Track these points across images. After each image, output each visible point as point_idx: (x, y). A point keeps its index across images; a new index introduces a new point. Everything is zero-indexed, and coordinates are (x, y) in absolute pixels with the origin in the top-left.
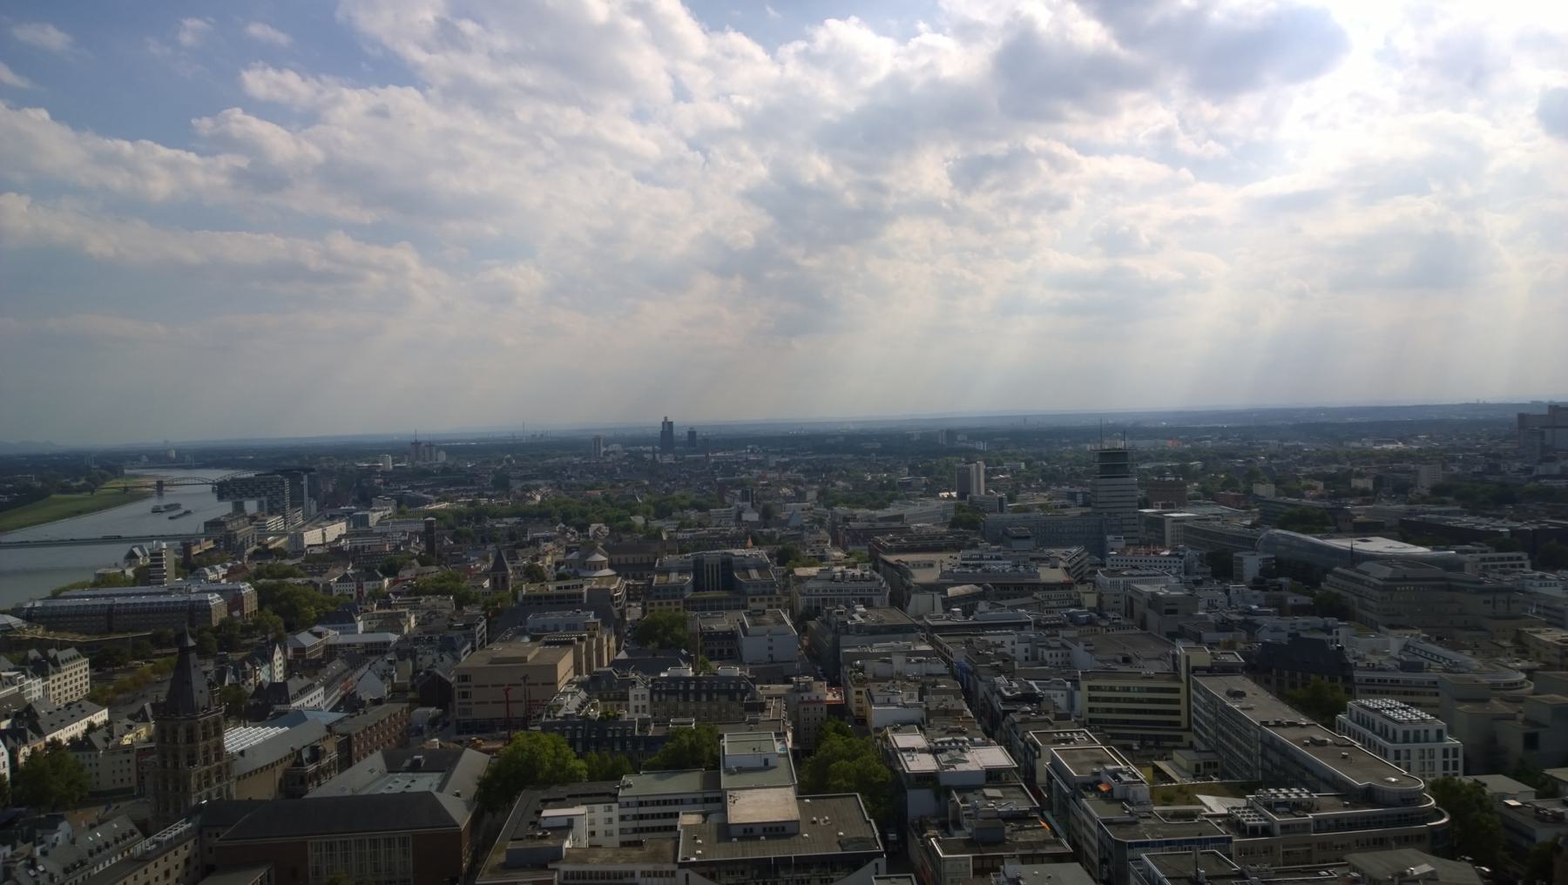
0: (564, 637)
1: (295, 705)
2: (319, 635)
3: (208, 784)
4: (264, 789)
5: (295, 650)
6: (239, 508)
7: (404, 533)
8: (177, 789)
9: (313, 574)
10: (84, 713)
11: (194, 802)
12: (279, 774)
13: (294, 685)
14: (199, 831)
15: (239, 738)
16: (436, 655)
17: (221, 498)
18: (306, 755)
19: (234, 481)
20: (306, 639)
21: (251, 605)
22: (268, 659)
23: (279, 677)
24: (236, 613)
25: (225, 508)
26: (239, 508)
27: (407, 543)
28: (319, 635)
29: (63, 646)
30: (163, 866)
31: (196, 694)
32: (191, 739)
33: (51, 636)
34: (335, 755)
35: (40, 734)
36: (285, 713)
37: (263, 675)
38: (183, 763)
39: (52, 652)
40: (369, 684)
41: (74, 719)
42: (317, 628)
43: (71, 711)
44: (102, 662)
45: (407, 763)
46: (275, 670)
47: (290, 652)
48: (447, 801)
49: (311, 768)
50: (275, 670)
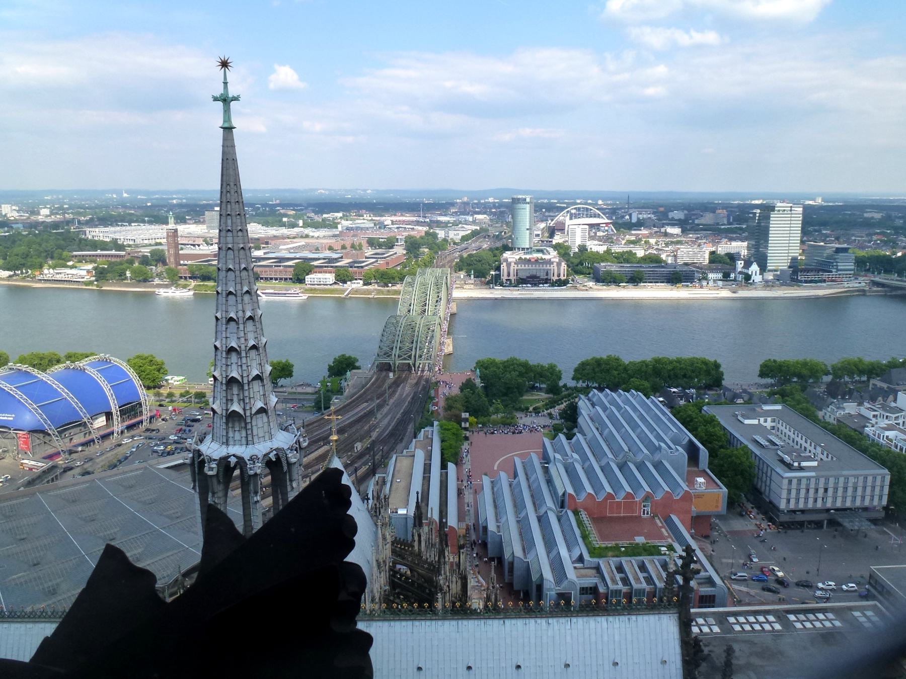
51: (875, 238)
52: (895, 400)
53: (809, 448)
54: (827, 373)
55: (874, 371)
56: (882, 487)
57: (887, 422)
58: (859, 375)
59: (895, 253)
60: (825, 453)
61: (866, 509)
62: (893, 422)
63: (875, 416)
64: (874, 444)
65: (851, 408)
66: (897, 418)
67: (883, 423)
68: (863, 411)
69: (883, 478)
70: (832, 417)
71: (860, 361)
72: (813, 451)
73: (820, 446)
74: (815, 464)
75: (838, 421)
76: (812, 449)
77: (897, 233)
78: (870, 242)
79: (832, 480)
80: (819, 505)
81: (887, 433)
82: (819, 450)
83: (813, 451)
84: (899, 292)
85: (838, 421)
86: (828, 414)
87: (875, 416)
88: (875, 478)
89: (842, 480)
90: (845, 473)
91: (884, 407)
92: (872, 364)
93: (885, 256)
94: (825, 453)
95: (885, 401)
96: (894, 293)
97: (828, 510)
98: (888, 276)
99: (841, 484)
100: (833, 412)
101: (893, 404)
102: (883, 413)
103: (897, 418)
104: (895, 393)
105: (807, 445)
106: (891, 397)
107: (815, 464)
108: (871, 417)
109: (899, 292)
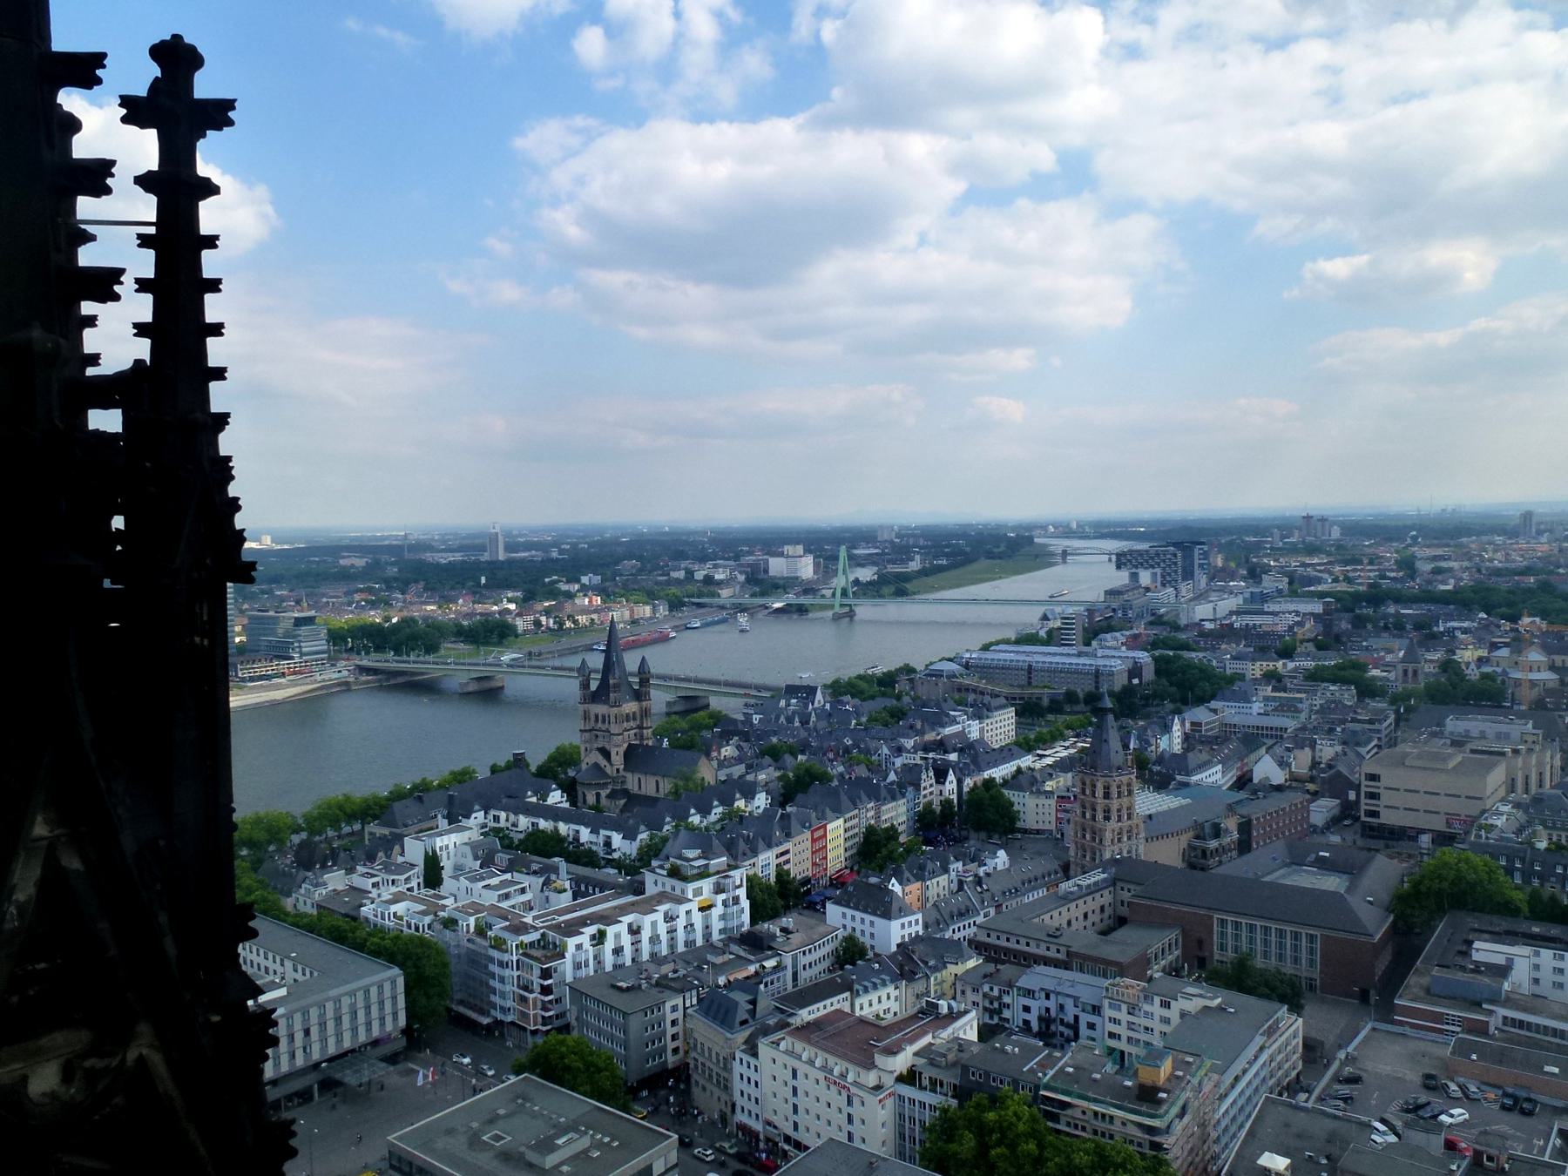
0: (1496, 747)
1: (1195, 778)
2: (1215, 711)
3: (1119, 840)
4: (1169, 853)
5: (1193, 724)
6: (1134, 577)
7: (1297, 613)
8: (1094, 839)
9: (1206, 650)
10: (1012, 757)
11: (1107, 855)
12: (1184, 845)
13: (1194, 758)
14: (1113, 882)
15: (1148, 802)
16: (1339, 748)
17: (1118, 567)
18: (1208, 829)
19: (1131, 552)
20: (1200, 714)
21: (1149, 674)
22: (1167, 729)
23: (1177, 748)
24: (1136, 681)
25: (1121, 578)
26: (1134, 577)
27: (1300, 624)
28: (1215, 711)
29: (995, 695)
30: (1083, 909)
31: (1113, 754)
32: (1107, 795)
33: (983, 684)
34: (1236, 836)
35: (980, 770)
36: (1186, 785)
37: (1163, 743)
38: (1100, 816)
39: (987, 698)
40: (1266, 769)
41: (1005, 761)
42: (1213, 704)
43: (1005, 754)
44: (1028, 711)
45: (1312, 857)
46: (1172, 741)
47: (1188, 725)
48: (1354, 901)
49: (1213, 844)
50: (1172, 741)
51: (357, 597)
52: (402, 854)
53: (272, 967)
54: (297, 830)
55: (374, 810)
56: (394, 998)
57: (394, 889)
58: (348, 824)
59: (387, 619)
60: (300, 968)
61: (375, 1043)
62: (402, 888)
63: (375, 885)
64: (379, 931)
65: (335, 880)
66: (408, 880)
67: (387, 893)
68: (357, 880)
69: (394, 982)
70: (309, 902)
71: (347, 798)
72: (280, 970)
73: (289, 958)
74: (282, 992)
75: (319, 907)
76: (277, 967)
77: (389, 588)
78: (349, 604)
79: (314, 1013)
80: (300, 1061)
81: (393, 908)
82: (289, 964)
83: (280, 970)
84: (400, 680)
85: (319, 907)
86: (301, 899)
87: (375, 885)
88: (381, 987)
89: (330, 1006)
90: (333, 993)
91: (387, 868)
92: (366, 800)
93: (373, 625)
94: (300, 968)
95: (389, 857)
96: (392, 682)
97: (317, 1066)
98: (379, 656)
99: (330, 1014)
100: (308, 894)
101: (400, 859)
102: (386, 876)
103: (408, 880)
104: (399, 839)
105: (269, 963)
106: (397, 848)
107: (282, 992)
108: (370, 888)
109: (400, 680)
